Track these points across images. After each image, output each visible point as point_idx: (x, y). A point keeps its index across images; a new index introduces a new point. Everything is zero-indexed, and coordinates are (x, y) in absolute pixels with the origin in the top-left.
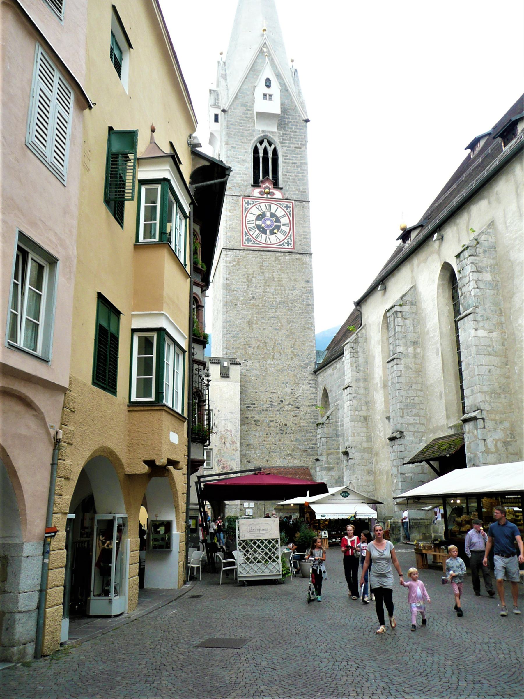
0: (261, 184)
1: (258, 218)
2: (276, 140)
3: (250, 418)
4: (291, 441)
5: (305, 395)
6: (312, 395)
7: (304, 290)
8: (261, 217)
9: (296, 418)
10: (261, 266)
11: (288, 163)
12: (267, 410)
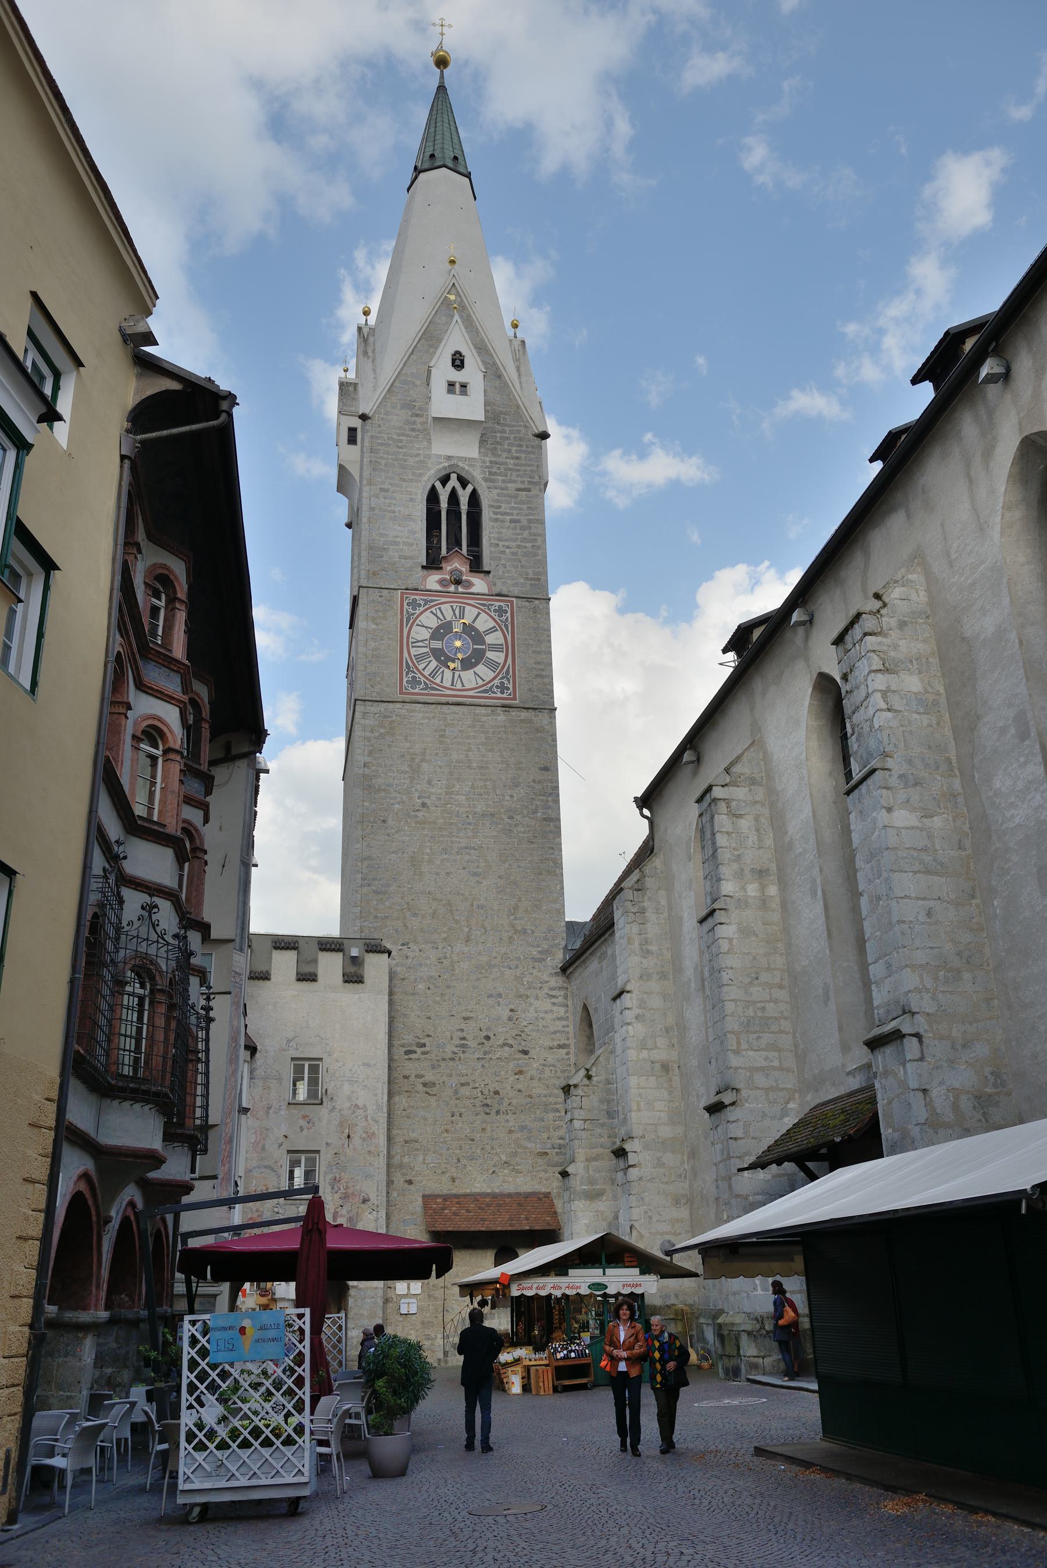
0: (443, 565)
2: (477, 476)
3: (412, 1078)
4: (510, 1132)
5: (541, 1023)
6: (558, 1023)
7: (538, 787)
8: (442, 631)
9: (521, 1078)
10: (441, 736)
11: (502, 521)
12: (452, 1059)
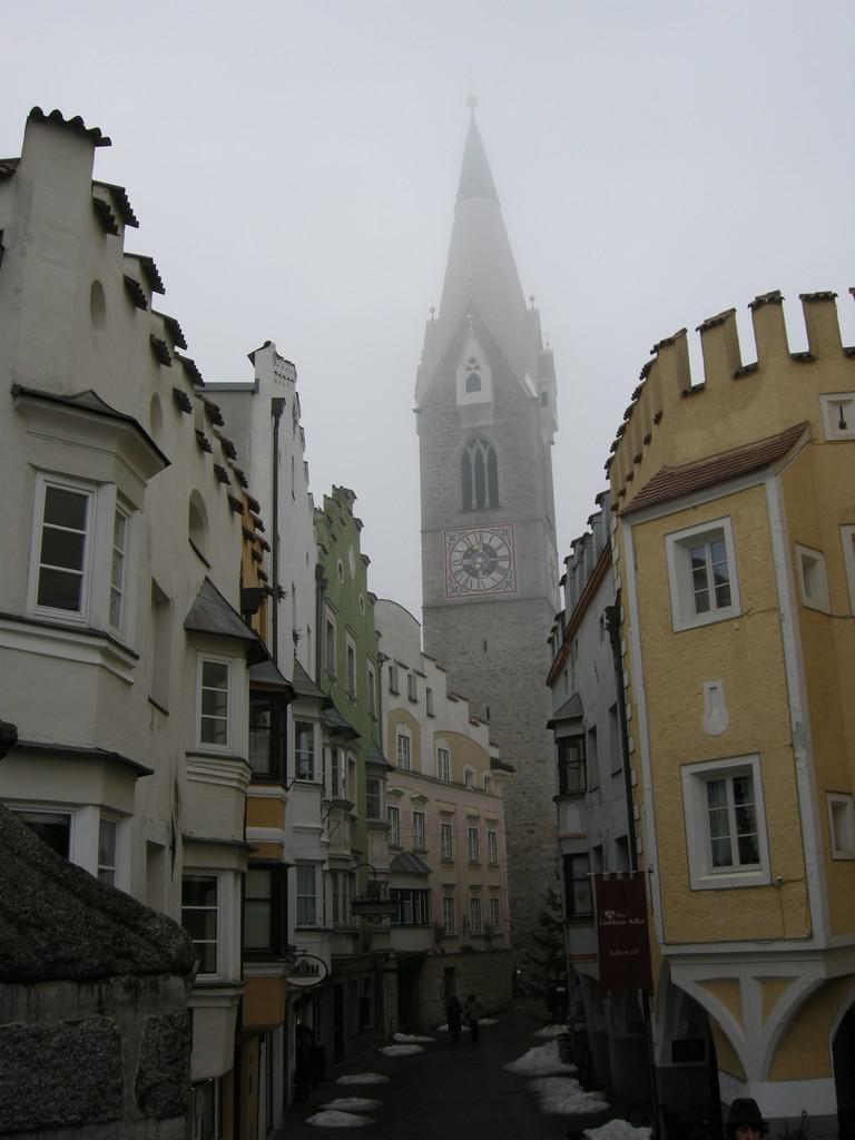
1: (466, 556)
